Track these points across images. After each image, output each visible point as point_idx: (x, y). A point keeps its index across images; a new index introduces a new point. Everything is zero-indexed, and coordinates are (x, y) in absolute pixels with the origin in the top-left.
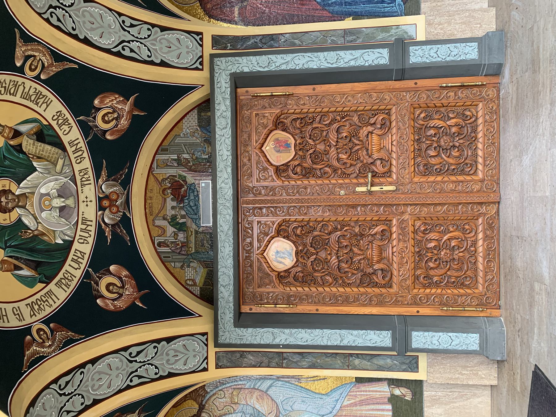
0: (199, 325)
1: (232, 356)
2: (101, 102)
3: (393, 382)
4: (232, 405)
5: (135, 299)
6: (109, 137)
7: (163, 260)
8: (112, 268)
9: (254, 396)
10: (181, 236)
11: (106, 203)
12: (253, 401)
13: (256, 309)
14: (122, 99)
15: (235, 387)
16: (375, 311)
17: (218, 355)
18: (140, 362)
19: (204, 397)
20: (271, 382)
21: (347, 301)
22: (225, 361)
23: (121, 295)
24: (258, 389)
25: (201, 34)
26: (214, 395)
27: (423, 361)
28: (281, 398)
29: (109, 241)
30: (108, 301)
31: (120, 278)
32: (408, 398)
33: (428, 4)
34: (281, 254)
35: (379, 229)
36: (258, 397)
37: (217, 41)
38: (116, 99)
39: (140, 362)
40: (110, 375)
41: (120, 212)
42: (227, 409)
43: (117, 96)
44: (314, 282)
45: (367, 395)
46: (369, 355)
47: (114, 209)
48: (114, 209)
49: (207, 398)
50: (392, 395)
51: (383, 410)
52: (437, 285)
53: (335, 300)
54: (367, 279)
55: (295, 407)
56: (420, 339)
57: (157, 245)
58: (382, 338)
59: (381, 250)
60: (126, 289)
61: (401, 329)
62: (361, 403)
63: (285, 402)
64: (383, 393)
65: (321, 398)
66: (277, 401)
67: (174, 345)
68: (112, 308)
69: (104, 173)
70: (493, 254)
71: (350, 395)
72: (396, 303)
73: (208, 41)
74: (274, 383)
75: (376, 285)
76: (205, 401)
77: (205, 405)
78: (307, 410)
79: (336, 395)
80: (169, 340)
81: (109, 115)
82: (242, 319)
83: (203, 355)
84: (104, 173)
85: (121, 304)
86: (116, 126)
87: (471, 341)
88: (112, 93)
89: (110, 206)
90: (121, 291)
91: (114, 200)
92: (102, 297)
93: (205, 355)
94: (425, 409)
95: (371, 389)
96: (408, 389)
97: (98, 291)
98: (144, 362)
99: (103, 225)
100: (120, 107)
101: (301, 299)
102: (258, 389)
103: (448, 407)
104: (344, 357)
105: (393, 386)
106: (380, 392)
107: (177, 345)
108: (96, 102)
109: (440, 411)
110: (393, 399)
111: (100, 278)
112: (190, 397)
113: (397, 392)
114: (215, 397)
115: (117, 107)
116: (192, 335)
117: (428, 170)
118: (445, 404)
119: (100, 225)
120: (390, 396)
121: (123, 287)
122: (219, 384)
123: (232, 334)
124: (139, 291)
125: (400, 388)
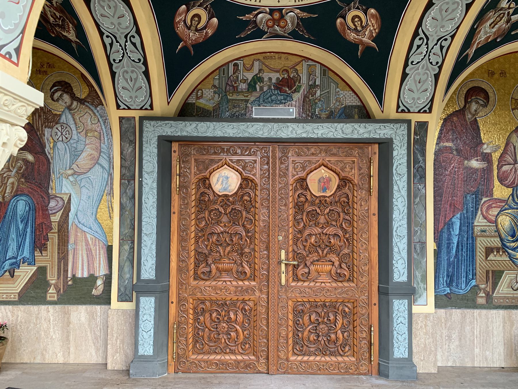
0: (161, 103)
1: (131, 133)
2: (373, 16)
4: (84, 131)
5: (186, 42)
6: (339, 21)
7: (222, 68)
8: (215, 20)
9: (93, 152)
10: (243, 86)
11: (277, 16)
12: (88, 151)
13: (175, 156)
14: (374, 35)
15: (102, 134)
16: (174, 264)
17: (132, 120)
18: (125, 46)
19: (92, 104)
20: (107, 168)
21: (182, 240)
22: (126, 126)
23: (189, 28)
24: (100, 155)
25: (430, 112)
26: (94, 113)
28: (92, 177)
29: (241, 18)
30: (183, 15)
31: (205, 28)
32: (94, 292)
33: (444, 315)
34: (226, 181)
35: (247, 269)
36: (93, 156)
37: (423, 126)
38: (375, 30)
39: (125, 46)
40: (113, 17)
41: (268, 29)
43: (377, 31)
44: (200, 210)
46: (132, 258)
47: (270, 24)
48: (270, 24)
49: (91, 107)
50: (97, 278)
51: (83, 269)
52: (196, 320)
53: (183, 230)
54: (201, 258)
55: (84, 190)
56: (148, 303)
57: (235, 63)
58: (149, 271)
59: (228, 271)
60: (195, 33)
61: (158, 288)
62: (89, 251)
63: (88, 180)
64: (98, 269)
65: (92, 214)
66: (89, 173)
67: (141, 78)
68: (177, 20)
69: (305, 15)
70: (223, 367)
71: (96, 240)
72: (180, 284)
73: (423, 117)
74: (106, 170)
75: (197, 266)
76: (88, 105)
77: (84, 104)
78: (81, 201)
79: (95, 227)
80: (146, 73)
81: (359, 23)
82: (165, 143)
83: (132, 105)
84: (305, 15)
85: (180, 28)
86: (349, 29)
87: (147, 348)
88: (380, 26)
89: (273, 20)
90: (193, 28)
91: (279, 23)
92: (188, 10)
93: (132, 108)
94: (84, 307)
95: (102, 259)
96: (103, 292)
97: (193, 6)
98: (126, 50)
99: (256, 12)
100: (366, 33)
102: (100, 155)
103: (87, 327)
104: (131, 234)
106: (99, 267)
107: (142, 81)
108: (373, 11)
109: (83, 319)
110: (92, 279)
111: (205, 8)
112: (92, 91)
113: (99, 282)
115: (367, 30)
116: (151, 95)
117: (298, 313)
118: (89, 324)
119: (256, 9)
120: (95, 275)
121: (197, 30)
122: (106, 121)
123: (152, 133)
124: (193, 46)
125: (103, 285)
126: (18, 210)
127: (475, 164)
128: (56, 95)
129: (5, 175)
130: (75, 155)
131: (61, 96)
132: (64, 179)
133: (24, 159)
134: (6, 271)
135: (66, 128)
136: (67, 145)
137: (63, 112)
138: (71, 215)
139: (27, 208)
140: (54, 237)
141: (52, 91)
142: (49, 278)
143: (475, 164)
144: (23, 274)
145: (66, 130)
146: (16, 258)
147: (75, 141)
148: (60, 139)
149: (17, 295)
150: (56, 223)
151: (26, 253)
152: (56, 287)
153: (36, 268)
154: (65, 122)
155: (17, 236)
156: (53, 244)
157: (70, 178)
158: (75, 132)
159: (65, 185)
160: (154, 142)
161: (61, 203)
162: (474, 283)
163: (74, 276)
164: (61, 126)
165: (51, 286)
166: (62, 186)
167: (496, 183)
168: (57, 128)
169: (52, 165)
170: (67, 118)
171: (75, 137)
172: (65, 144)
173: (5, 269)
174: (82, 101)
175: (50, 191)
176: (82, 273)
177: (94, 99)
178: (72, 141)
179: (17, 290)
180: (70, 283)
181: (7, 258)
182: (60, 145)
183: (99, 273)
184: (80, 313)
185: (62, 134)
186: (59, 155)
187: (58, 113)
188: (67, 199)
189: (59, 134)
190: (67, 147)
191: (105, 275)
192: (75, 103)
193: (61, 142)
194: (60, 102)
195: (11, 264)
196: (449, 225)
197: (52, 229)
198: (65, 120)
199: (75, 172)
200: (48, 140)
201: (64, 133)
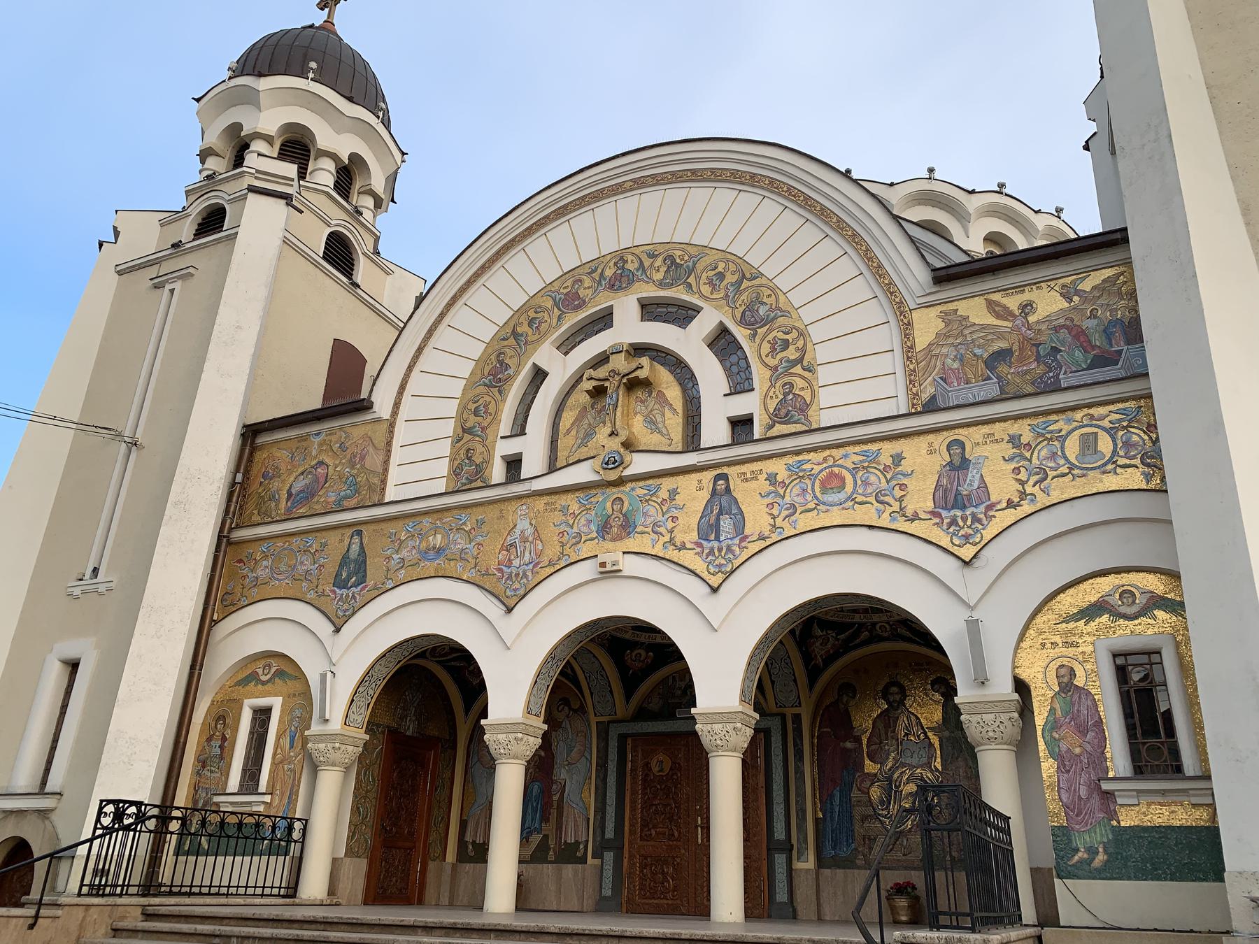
0: (622, 709)
3: (587, 841)
7: (664, 681)
13: (629, 747)
16: (626, 829)
21: (633, 809)
27: (597, 861)
35: (676, 834)
37: (797, 718)
44: (644, 789)
46: (601, 826)
52: (641, 871)
53: (633, 802)
54: (645, 825)
56: (609, 856)
58: (610, 834)
61: (615, 846)
62: (575, 821)
73: (796, 710)
75: (642, 830)
79: (581, 804)
80: (611, 692)
82: (623, 738)
87: (608, 892)
94: (570, 866)
101: (634, 778)
104: (601, 810)
107: (609, 697)
110: (577, 843)
123: (614, 733)
127: (848, 745)
130: (570, 751)
140: (554, 812)
143: (848, 745)
151: (537, 825)
160: (616, 737)
162: (853, 846)
166: (561, 774)
167: (867, 762)
170: (566, 724)
174: (575, 711)
176: (571, 840)
177: (582, 710)
184: (569, 870)
186: (560, 750)
196: (832, 796)
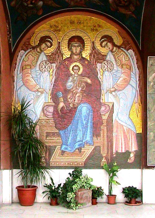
9: (126, 77)
19: (125, 48)
20: (135, 87)
26: (127, 55)
28: (126, 92)
32: (129, 161)
42: (119, 62)
45: (130, 139)
49: (124, 50)
50: (130, 153)
51: (122, 148)
71: (129, 130)
74: (135, 89)
77: (120, 49)
78: (120, 107)
102: (130, 79)
105: (135, 153)
106: (132, 146)
110: (128, 153)
114: (125, 55)
125: (134, 157)
126: (83, 113)
128: (104, 44)
129: (74, 92)
131: (106, 44)
132: (109, 93)
133: (85, 82)
134: (76, 149)
135: (110, 63)
136: (111, 73)
137: (108, 53)
138: (114, 115)
139: (88, 111)
140: (104, 128)
141: (101, 41)
142: (102, 153)
144: (86, 151)
145: (110, 64)
146: (82, 141)
147: (116, 71)
148: (107, 70)
149: (83, 163)
150: (106, 120)
151: (88, 138)
152: (106, 158)
153: (94, 147)
154: (109, 60)
155: (82, 128)
156: (103, 132)
157: (113, 93)
158: (115, 66)
159: (110, 97)
161: (108, 108)
163: (117, 151)
164: (107, 62)
165: (103, 158)
168: (104, 63)
169: (102, 85)
171: (115, 68)
172: (110, 73)
173: (76, 148)
174: (119, 47)
175: (101, 101)
176: (122, 149)
178: (114, 71)
179: (83, 160)
180: (114, 156)
181: (77, 141)
182: (106, 73)
183: (132, 150)
185: (108, 67)
187: (106, 54)
188: (112, 105)
189: (106, 67)
190: (111, 74)
191: (135, 151)
192: (115, 48)
193: (107, 72)
194: (106, 47)
195: (79, 145)
197: (103, 124)
198: (109, 58)
199: (116, 89)
200: (99, 70)
201: (109, 66)
